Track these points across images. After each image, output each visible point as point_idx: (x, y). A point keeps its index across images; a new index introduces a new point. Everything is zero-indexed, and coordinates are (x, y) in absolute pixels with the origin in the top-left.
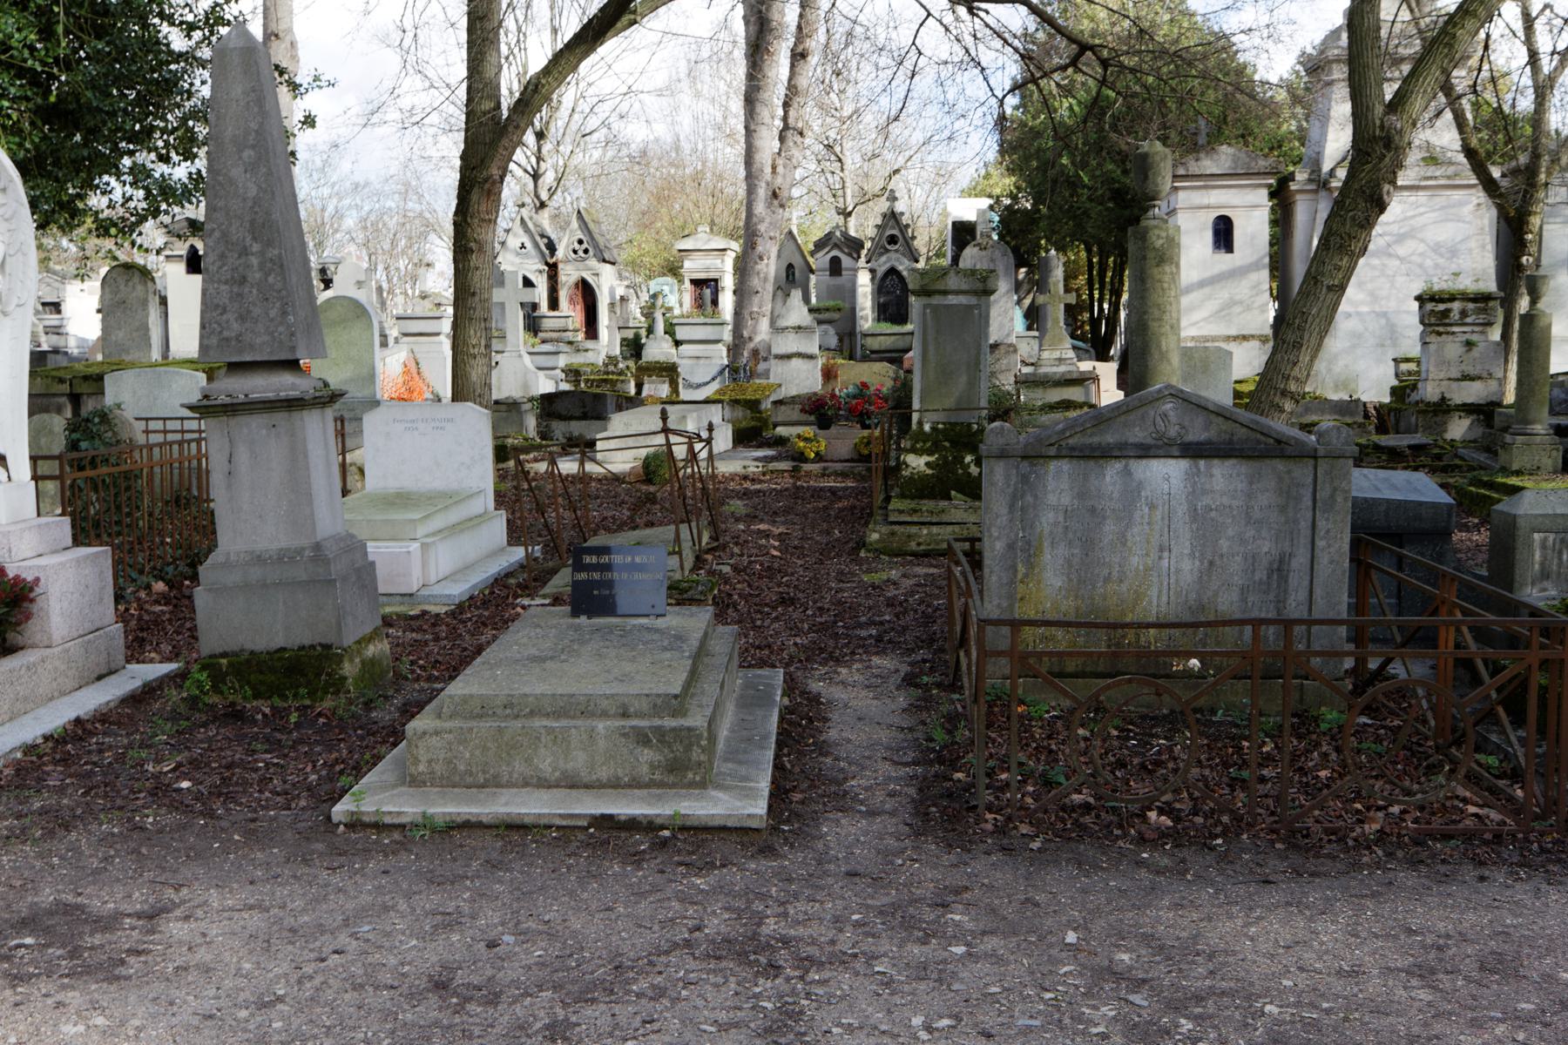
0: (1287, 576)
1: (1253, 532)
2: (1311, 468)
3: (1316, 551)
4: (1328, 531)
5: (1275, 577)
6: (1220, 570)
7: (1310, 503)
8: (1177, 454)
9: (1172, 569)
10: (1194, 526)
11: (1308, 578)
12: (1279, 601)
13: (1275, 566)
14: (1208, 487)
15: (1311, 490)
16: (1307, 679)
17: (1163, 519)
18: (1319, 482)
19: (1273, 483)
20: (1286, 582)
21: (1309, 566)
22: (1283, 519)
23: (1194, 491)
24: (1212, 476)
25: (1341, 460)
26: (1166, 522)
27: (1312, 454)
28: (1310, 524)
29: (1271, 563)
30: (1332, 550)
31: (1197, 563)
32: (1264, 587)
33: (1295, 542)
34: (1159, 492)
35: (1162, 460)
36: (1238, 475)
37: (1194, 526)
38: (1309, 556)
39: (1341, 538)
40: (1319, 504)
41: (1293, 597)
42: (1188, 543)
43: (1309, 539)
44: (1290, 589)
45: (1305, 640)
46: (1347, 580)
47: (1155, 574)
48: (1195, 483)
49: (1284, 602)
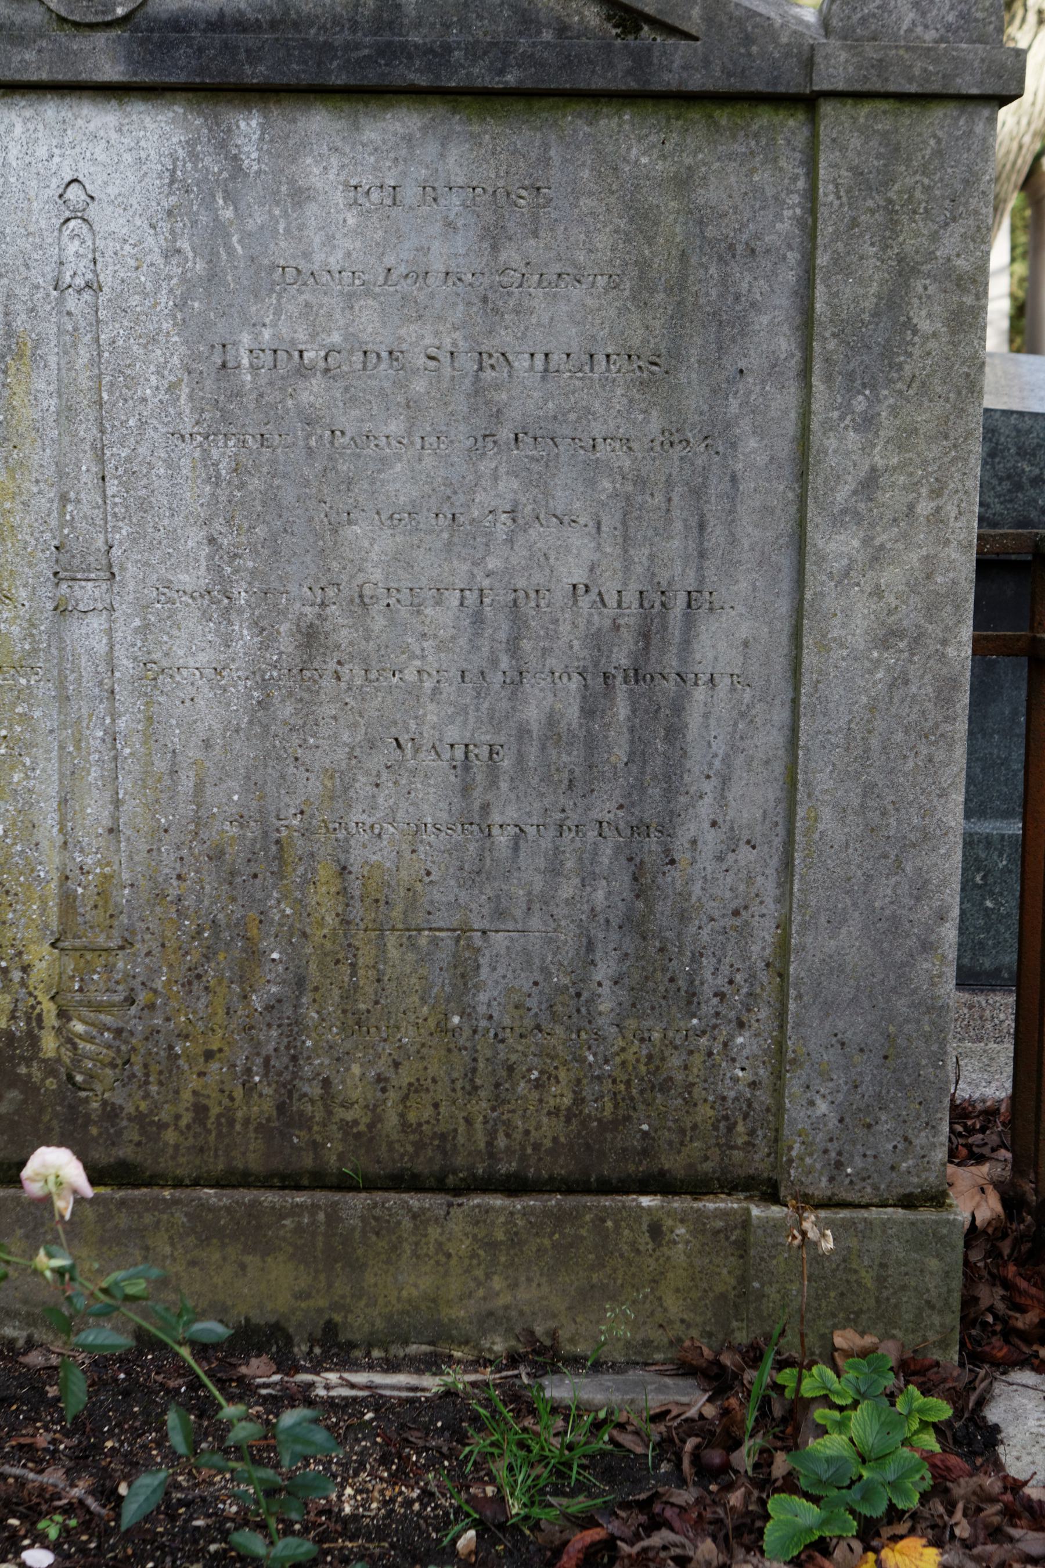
0: (678, 708)
1: (509, 486)
2: (791, 164)
3: (816, 581)
4: (870, 484)
5: (622, 710)
6: (353, 672)
7: (785, 344)
8: (111, 72)
9: (125, 664)
10: (223, 452)
11: (781, 715)
12: (639, 829)
13: (622, 657)
14: (283, 250)
15: (789, 276)
16: (771, 1195)
17: (67, 413)
18: (826, 230)
19: (602, 241)
20: (674, 733)
21: (780, 665)
22: (655, 425)
23: (213, 276)
24: (300, 196)
25: (939, 114)
26: (87, 431)
27: (792, 83)
28: (785, 449)
29: (597, 642)
30: (892, 577)
31: (245, 636)
32: (570, 758)
33: (716, 535)
34: (42, 276)
35: (52, 110)
36: (430, 192)
37: (223, 452)
38: (783, 606)
39: (937, 517)
40: (826, 344)
41: (706, 809)
42: (194, 538)
43: (784, 525)
44: (695, 763)
45: (763, 1013)
46: (962, 726)
47: (45, 690)
48: (220, 230)
49: (666, 831)
